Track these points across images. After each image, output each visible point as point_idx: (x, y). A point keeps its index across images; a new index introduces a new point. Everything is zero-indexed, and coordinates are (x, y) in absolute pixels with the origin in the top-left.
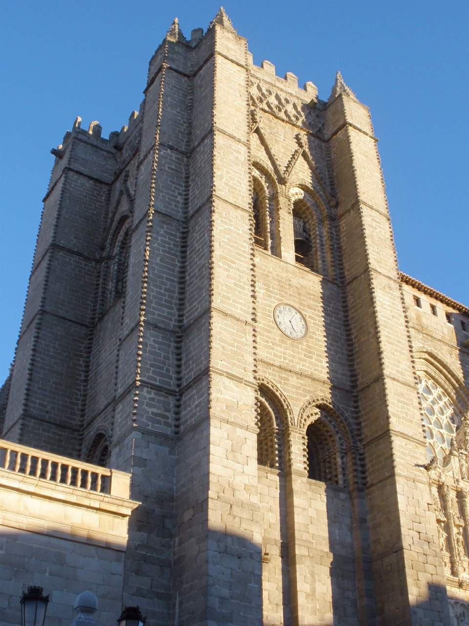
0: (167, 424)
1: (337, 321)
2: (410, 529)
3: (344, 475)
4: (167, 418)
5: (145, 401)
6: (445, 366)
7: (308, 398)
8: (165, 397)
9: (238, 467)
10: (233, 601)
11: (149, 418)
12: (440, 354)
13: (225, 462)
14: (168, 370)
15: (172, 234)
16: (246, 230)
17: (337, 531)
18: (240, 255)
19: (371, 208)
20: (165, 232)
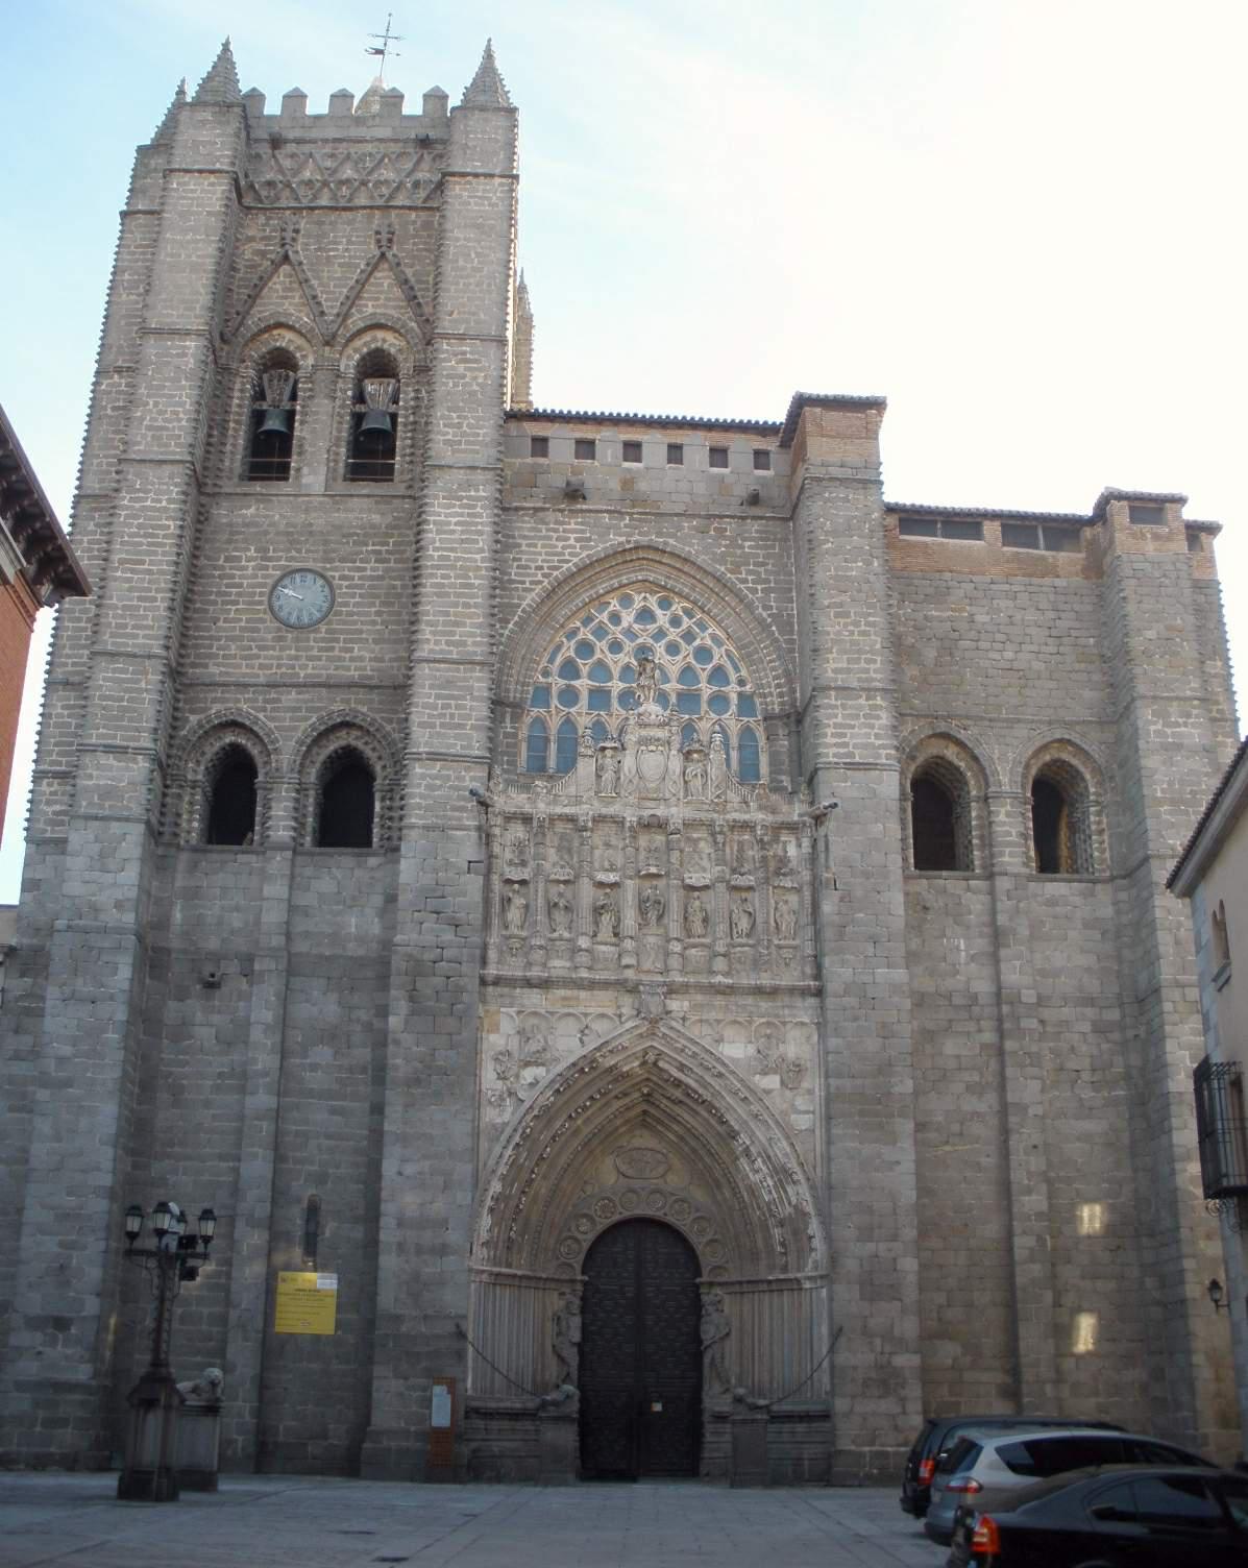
1: (400, 566)
6: (686, 560)
7: (314, 719)
9: (109, 878)
12: (671, 541)
20: (96, 525)
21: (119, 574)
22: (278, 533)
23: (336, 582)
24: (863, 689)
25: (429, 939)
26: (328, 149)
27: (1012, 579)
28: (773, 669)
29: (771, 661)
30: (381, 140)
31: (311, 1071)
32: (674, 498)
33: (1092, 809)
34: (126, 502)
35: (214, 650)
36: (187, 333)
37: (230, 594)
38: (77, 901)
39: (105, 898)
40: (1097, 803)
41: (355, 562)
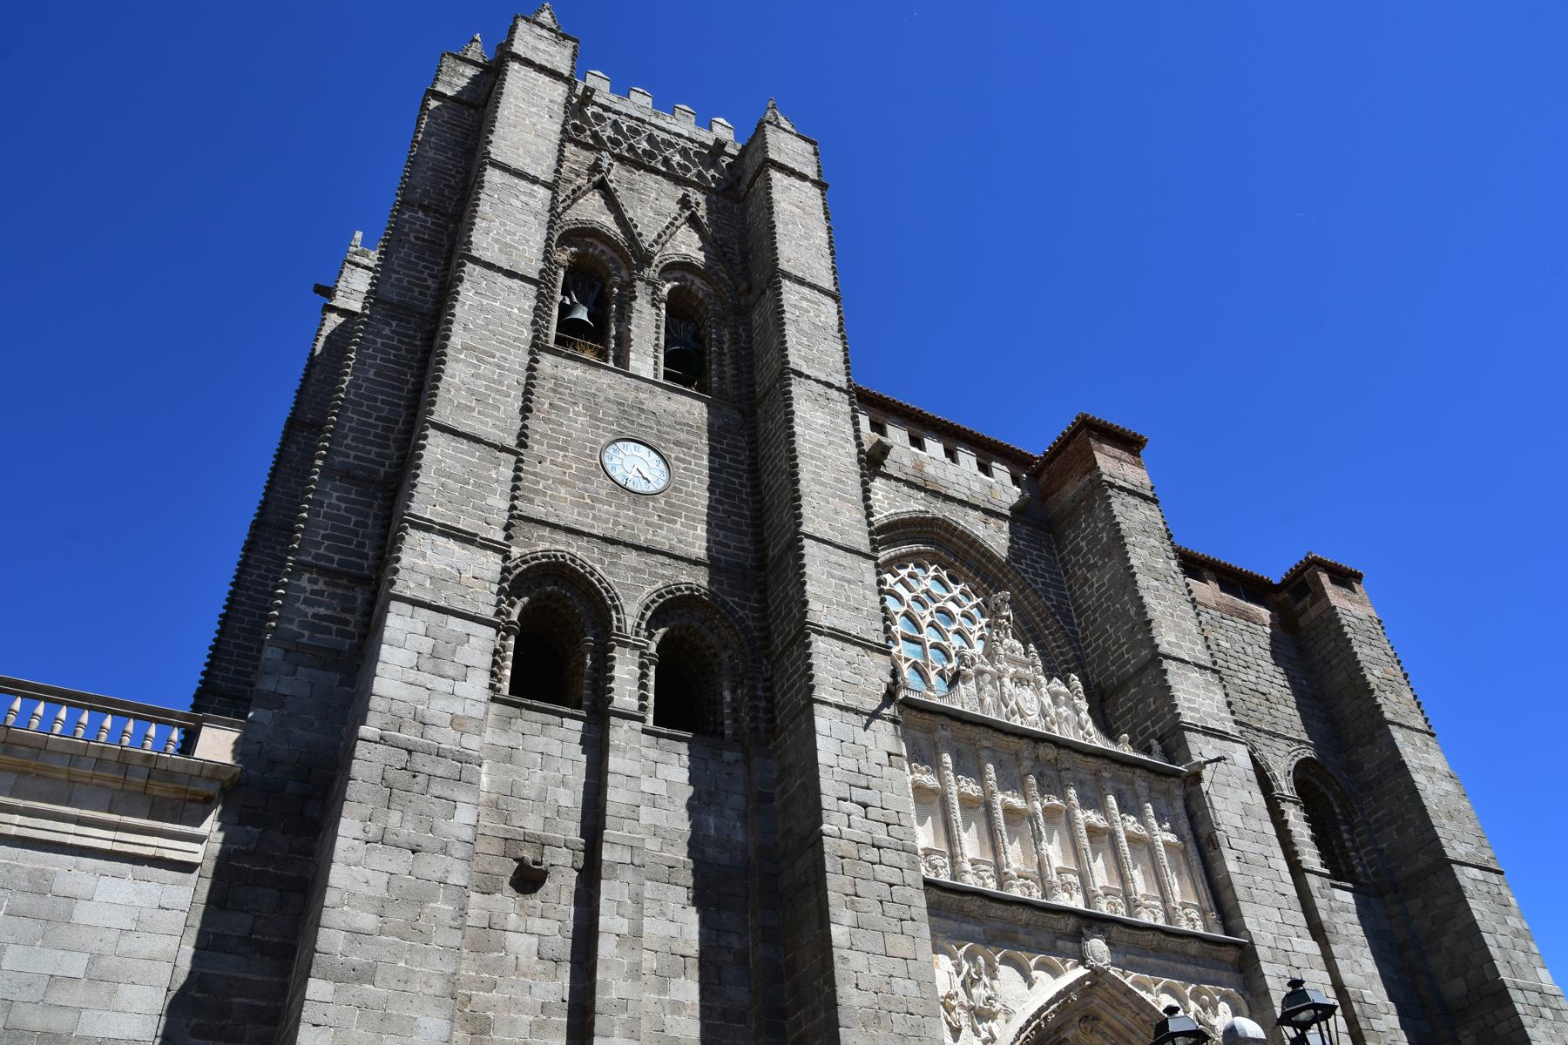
0: (343, 634)
2: (845, 800)
3: (735, 720)
4: (347, 623)
5: (302, 596)
7: (660, 585)
8: (346, 587)
9: (443, 685)
10: (383, 937)
11: (303, 625)
12: (962, 522)
13: (413, 675)
14: (361, 545)
15: (406, 335)
16: (527, 308)
17: (711, 821)
18: (507, 344)
19: (801, 282)
20: (392, 332)
21: (462, 356)
22: (608, 400)
23: (672, 461)
24: (1197, 665)
25: (856, 833)
26: (633, 123)
27: (1234, 618)
28: (1062, 654)
29: (1058, 647)
30: (680, 136)
31: (673, 1013)
32: (957, 487)
33: (1343, 828)
34: (471, 294)
35: (541, 487)
36: (534, 181)
37: (557, 440)
38: (395, 706)
39: (438, 709)
40: (1347, 823)
41: (690, 449)
